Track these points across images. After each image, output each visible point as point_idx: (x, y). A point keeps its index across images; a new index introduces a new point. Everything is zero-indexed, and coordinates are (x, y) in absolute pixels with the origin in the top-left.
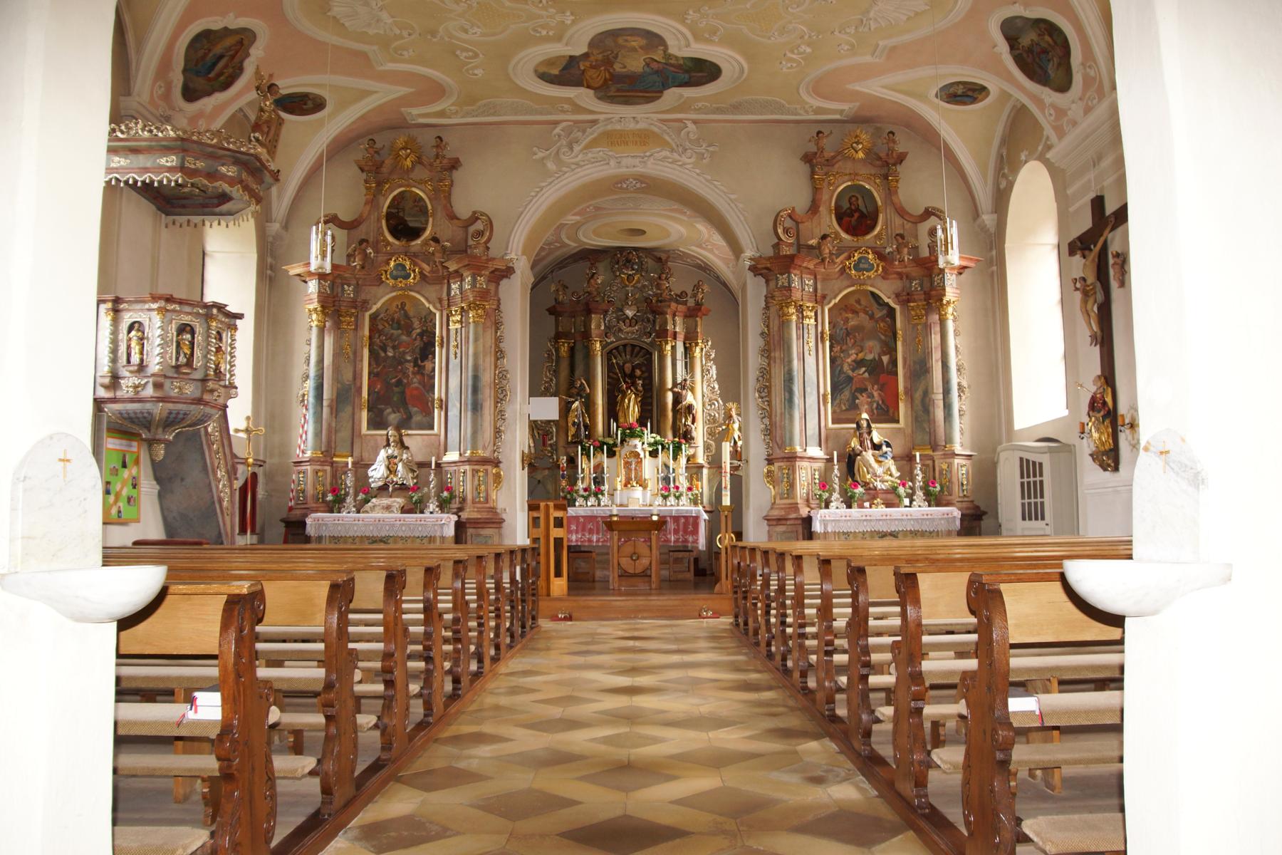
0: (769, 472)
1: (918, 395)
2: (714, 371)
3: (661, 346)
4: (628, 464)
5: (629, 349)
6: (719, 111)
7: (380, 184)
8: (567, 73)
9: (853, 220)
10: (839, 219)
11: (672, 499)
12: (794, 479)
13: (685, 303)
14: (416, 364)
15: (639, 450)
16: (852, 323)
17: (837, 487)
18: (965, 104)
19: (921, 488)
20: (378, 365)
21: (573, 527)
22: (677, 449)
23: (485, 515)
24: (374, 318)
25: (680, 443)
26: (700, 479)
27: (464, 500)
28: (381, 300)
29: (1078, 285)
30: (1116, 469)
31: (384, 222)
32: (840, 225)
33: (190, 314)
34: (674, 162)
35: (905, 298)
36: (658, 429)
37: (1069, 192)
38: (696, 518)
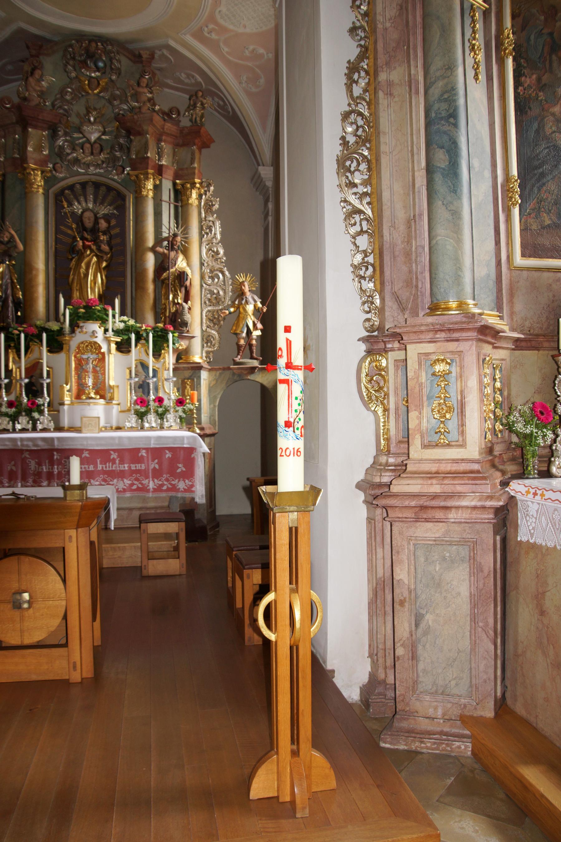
2: (217, 229)
5: (90, 190)
13: (177, 122)
15: (100, 339)
26: (196, 386)
36: (132, 309)
38: (191, 450)
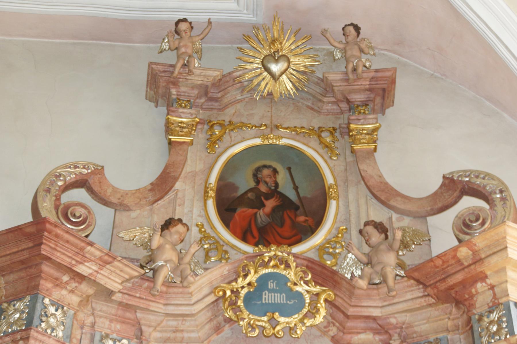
9: (262, 215)
32: (226, 222)
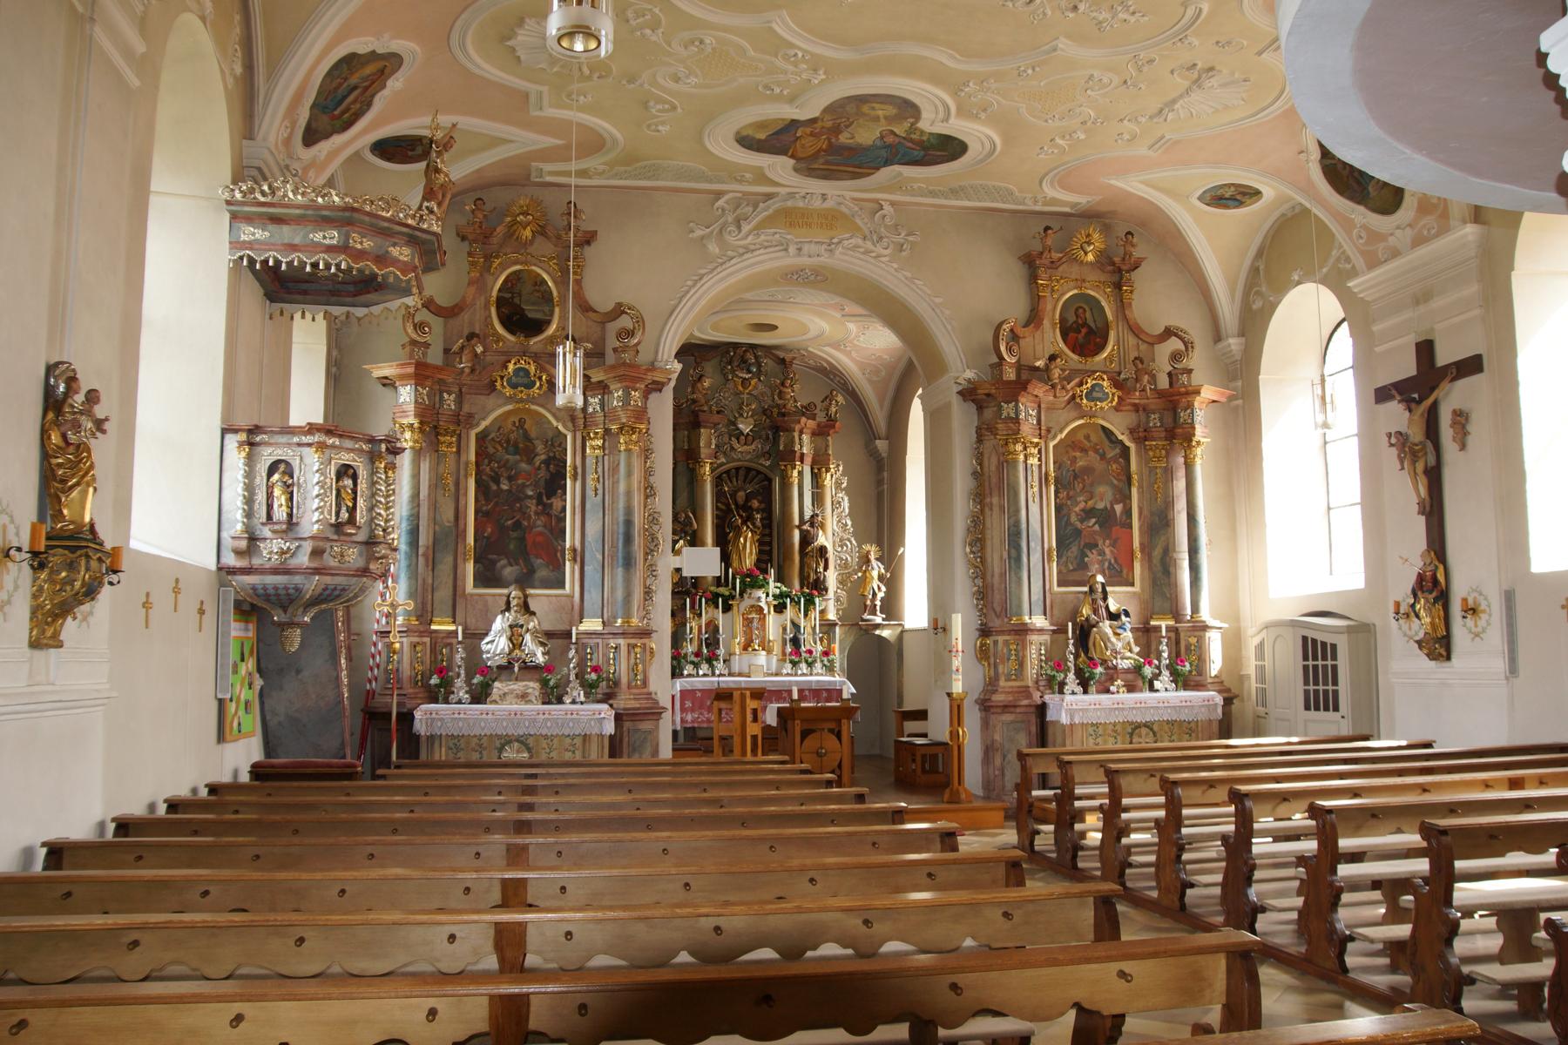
0: (982, 645)
1: (1157, 553)
2: (846, 504)
3: (785, 470)
4: (748, 622)
5: (742, 472)
6: (933, 194)
7: (488, 258)
8: (777, 139)
10: (1065, 335)
11: (803, 665)
12: (1024, 656)
14: (540, 502)
15: (763, 604)
16: (1081, 463)
17: (1071, 665)
18: (1226, 207)
19: (1167, 667)
20: (488, 500)
21: (688, 704)
22: (810, 602)
23: (644, 704)
24: (481, 438)
25: (811, 595)
27: (617, 683)
28: (493, 413)
29: (1393, 440)
30: (1448, 658)
31: (493, 310)
33: (352, 450)
34: (867, 252)
35: (1141, 435)
37: (1376, 328)
